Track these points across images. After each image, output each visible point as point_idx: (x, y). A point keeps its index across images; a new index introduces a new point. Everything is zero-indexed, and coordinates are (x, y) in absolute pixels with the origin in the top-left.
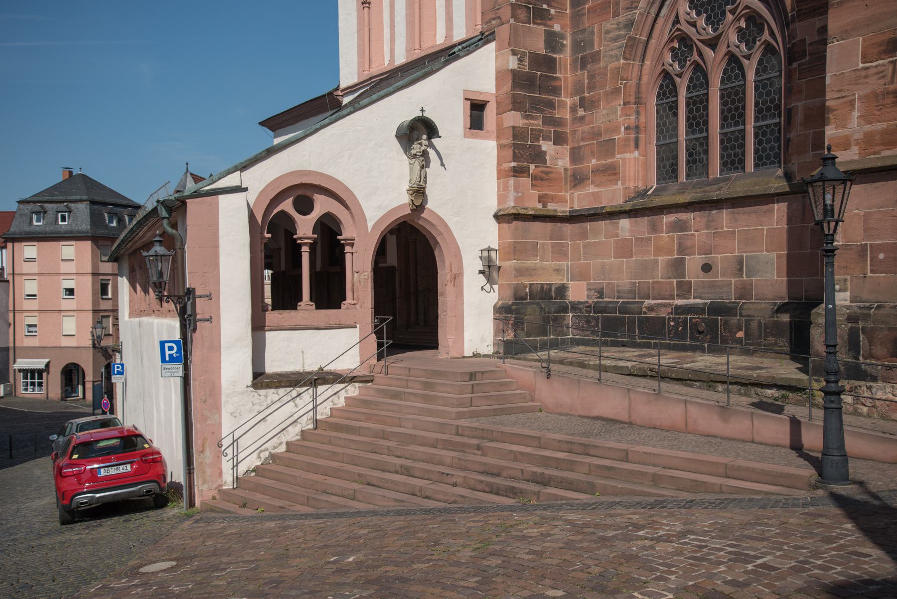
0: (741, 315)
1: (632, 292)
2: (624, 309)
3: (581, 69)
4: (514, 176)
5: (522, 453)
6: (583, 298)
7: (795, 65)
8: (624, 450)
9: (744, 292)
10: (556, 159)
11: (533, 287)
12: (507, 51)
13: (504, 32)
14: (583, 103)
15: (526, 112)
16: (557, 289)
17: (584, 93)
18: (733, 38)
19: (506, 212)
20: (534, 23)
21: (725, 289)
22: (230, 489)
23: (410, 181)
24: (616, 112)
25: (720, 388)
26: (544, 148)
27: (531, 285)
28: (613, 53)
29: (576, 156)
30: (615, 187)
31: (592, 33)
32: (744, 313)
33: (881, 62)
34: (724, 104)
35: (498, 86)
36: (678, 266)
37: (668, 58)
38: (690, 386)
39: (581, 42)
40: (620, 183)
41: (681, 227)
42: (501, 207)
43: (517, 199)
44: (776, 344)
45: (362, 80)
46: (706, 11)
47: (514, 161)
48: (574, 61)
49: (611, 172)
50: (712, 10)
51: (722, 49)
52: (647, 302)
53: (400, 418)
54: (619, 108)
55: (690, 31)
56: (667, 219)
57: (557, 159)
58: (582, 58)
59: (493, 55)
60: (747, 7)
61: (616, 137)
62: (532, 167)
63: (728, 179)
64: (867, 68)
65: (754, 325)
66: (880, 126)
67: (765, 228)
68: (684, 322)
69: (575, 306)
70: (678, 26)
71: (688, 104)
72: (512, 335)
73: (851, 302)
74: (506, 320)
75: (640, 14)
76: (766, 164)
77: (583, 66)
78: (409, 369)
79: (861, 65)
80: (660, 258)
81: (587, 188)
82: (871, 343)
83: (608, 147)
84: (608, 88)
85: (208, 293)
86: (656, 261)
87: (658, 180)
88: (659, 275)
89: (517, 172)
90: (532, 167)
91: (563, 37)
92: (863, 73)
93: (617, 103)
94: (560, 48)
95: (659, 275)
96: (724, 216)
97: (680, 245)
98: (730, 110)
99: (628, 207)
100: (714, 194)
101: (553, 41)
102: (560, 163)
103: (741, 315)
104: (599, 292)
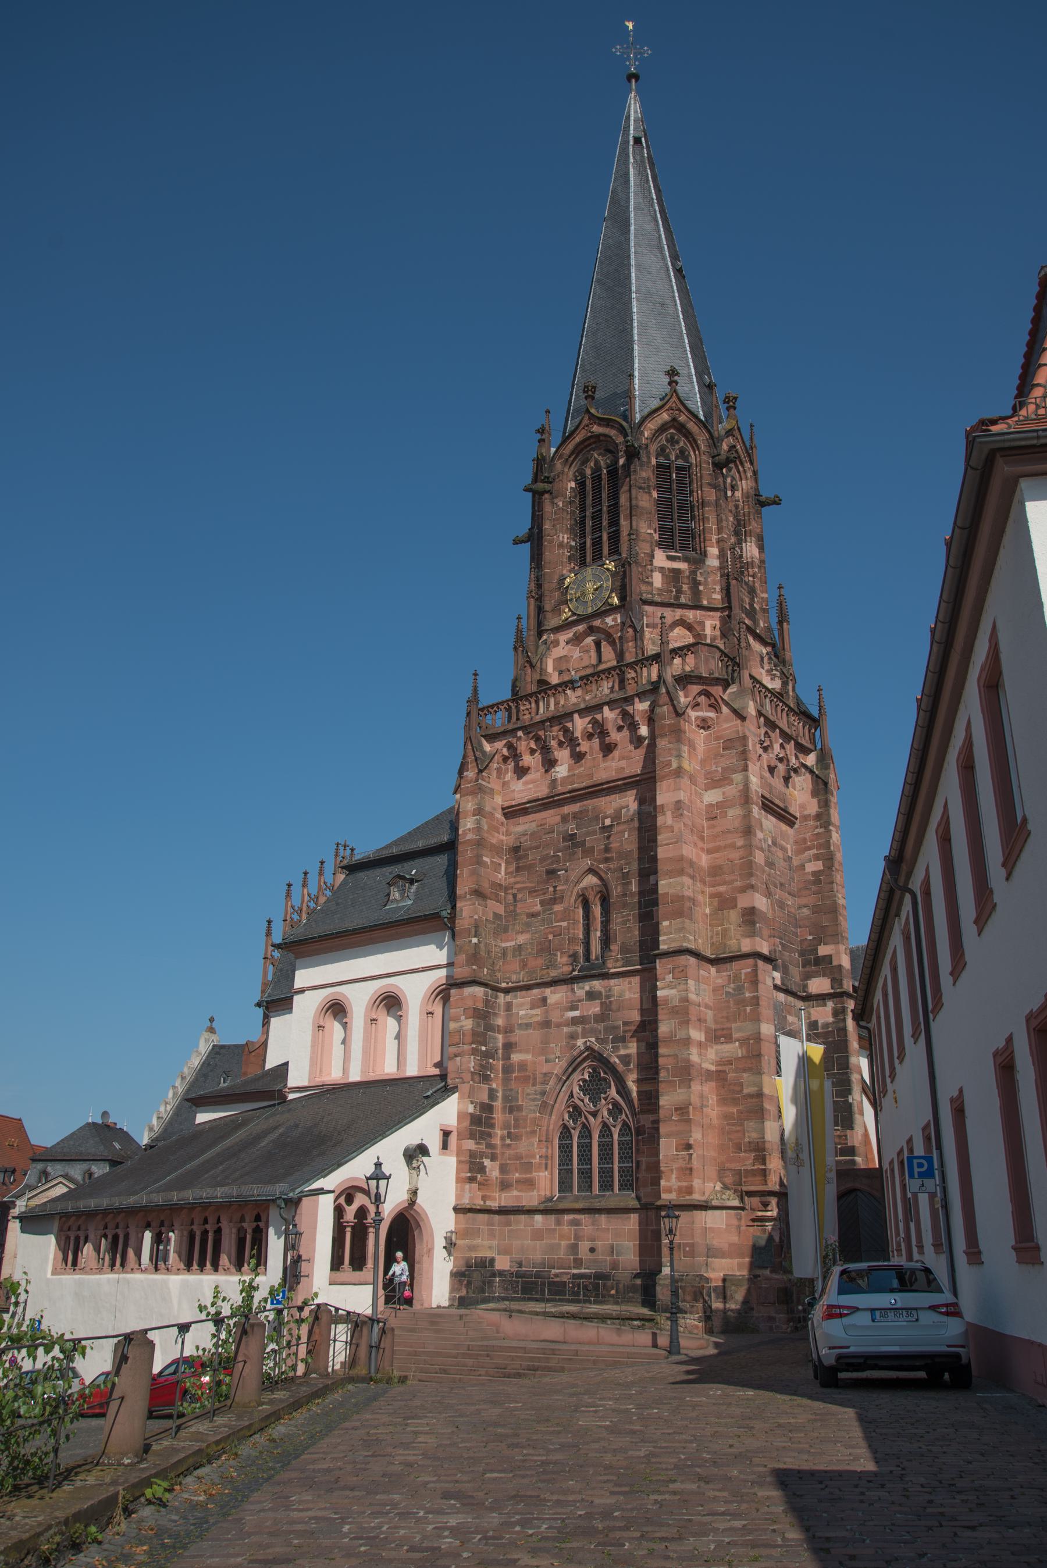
14: (509, 1135)
18: (606, 1114)
24: (533, 1145)
28: (532, 1108)
37: (566, 1117)
46: (589, 1094)
48: (504, 1108)
51: (600, 1119)
55: (580, 1104)
58: (510, 1106)
77: (511, 1112)
91: (497, 1091)
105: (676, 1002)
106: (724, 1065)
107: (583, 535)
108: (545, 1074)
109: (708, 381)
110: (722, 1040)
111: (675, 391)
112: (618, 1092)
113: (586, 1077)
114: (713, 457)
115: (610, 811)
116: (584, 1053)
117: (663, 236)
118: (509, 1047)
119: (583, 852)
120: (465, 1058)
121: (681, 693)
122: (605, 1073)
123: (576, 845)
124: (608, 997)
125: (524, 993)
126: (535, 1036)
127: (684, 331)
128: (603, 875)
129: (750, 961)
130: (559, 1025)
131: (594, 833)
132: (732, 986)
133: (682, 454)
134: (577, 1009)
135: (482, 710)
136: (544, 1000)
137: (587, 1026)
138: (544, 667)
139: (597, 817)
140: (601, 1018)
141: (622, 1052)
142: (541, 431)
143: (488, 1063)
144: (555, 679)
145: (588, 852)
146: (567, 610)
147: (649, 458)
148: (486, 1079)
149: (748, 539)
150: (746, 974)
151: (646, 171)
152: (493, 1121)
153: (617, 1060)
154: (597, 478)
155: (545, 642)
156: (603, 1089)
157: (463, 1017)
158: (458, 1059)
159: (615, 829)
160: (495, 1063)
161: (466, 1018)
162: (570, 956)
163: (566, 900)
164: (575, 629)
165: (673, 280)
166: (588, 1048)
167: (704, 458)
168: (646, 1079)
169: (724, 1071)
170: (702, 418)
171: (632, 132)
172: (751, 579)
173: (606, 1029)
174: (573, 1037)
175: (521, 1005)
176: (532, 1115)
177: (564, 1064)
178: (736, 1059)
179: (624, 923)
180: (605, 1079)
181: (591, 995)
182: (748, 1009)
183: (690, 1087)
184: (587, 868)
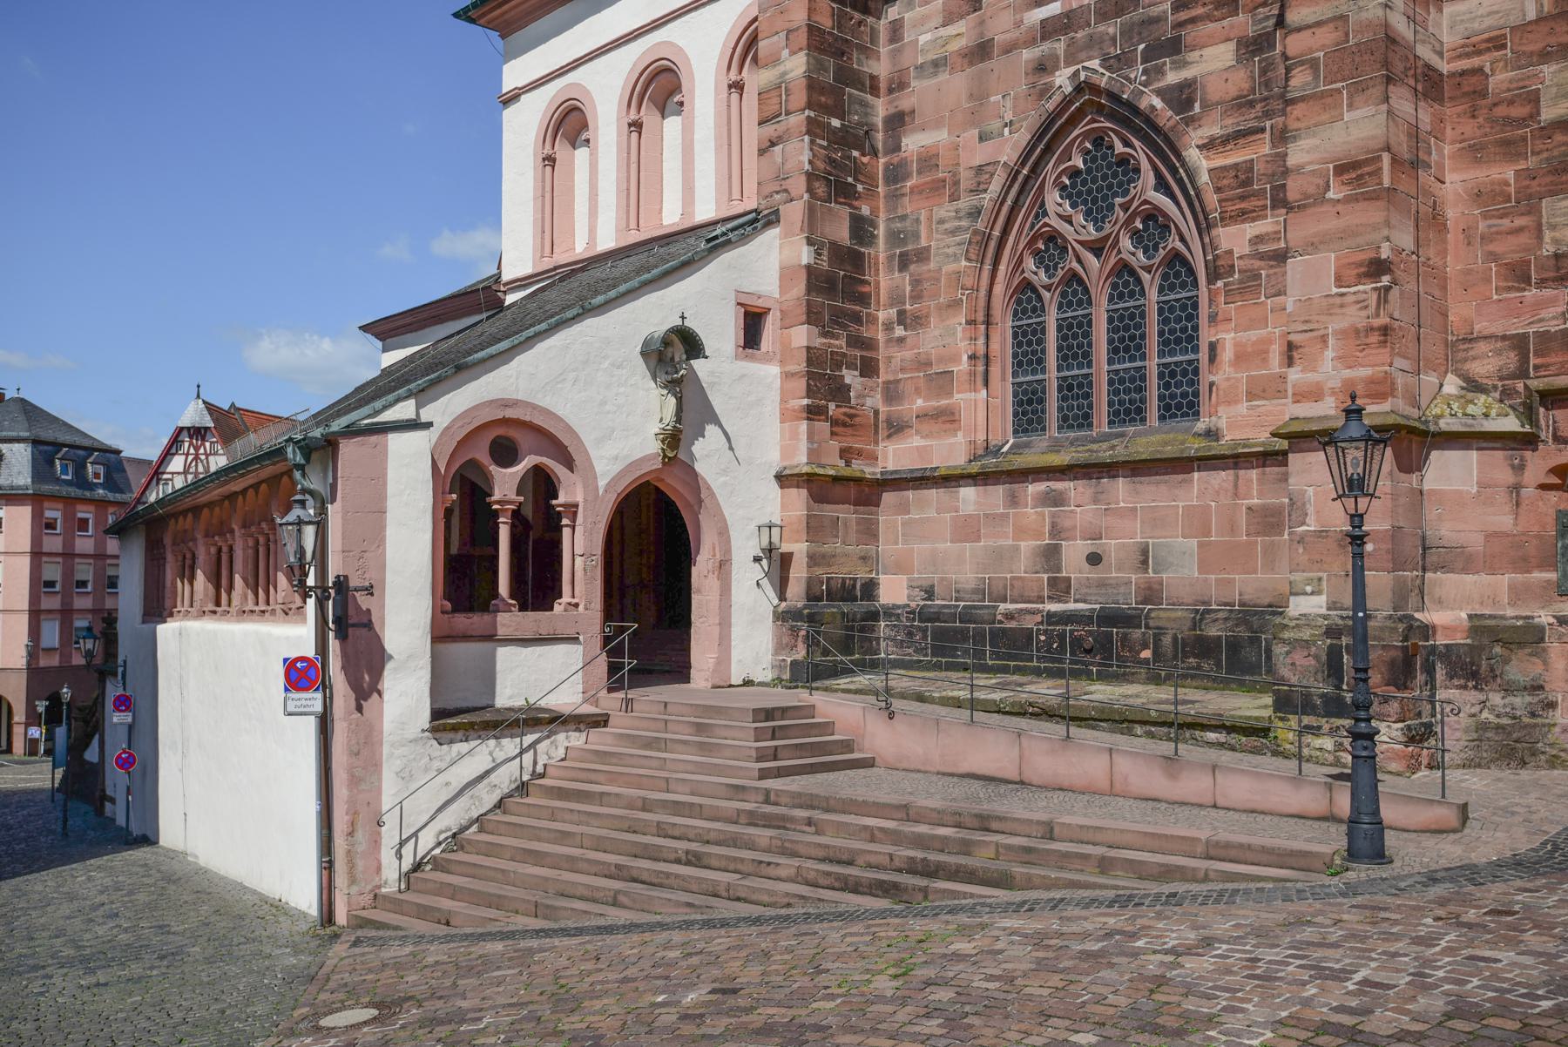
0: (1147, 627)
1: (979, 592)
2: (967, 616)
3: (900, 270)
4: (808, 419)
5: (881, 829)
6: (901, 599)
7: (1220, 284)
8: (1039, 823)
9: (1151, 594)
11: (832, 582)
13: (794, 212)
14: (902, 318)
15: (823, 327)
16: (862, 585)
17: (904, 303)
19: (796, 471)
20: (836, 202)
21: (1122, 590)
22: (394, 893)
23: (661, 420)
24: (954, 334)
25: (1139, 730)
26: (848, 380)
27: (828, 579)
28: (950, 251)
30: (952, 440)
31: (918, 221)
32: (1151, 623)
33: (1361, 288)
34: (1113, 330)
35: (783, 288)
36: (1051, 555)
37: (1030, 263)
38: (1093, 728)
39: (900, 232)
40: (960, 434)
41: (1056, 500)
42: (786, 463)
43: (813, 454)
44: (1199, 667)
45: (540, 270)
46: (1085, 202)
47: (808, 397)
48: (890, 258)
49: (947, 418)
50: (1094, 201)
52: (1003, 607)
53: (667, 780)
54: (960, 329)
56: (1034, 489)
57: (864, 396)
58: (901, 255)
59: (777, 242)
60: (1146, 202)
61: (955, 369)
62: (832, 406)
63: (1122, 435)
64: (1343, 295)
65: (1167, 640)
66: (1364, 372)
67: (1181, 504)
68: (1062, 636)
69: (890, 612)
70: (1046, 220)
71: (1059, 328)
72: (804, 653)
73: (1329, 609)
74: (794, 631)
75: (991, 200)
76: (1176, 416)
78: (666, 704)
79: (1335, 290)
80: (1022, 544)
81: (910, 440)
83: (942, 383)
84: (941, 300)
85: (367, 584)
86: (1017, 548)
87: (1015, 432)
89: (813, 413)
90: (832, 406)
91: (874, 225)
92: (1338, 300)
93: (956, 320)
94: (871, 239)
95: (1023, 566)
96: (1120, 488)
97: (1054, 525)
98: (1122, 340)
99: (975, 468)
101: (861, 229)
102: (869, 402)
103: (1147, 627)
104: (926, 592)
106: (1479, 53)
108: (979, 169)
112: (1162, 185)
113: (1078, 162)
116: (1071, 102)
118: (898, 122)
122: (1127, 144)
130: (1009, 49)
137: (1080, 34)
141: (1172, 78)
143: (849, 157)
148: (843, 192)
152: (865, 289)
153: (1157, 102)
156: (1120, 185)
160: (865, 160)
161: (793, 53)
166: (1079, 89)
169: (1479, 71)
173: (1127, 32)
174: (1043, 67)
176: (950, 267)
177: (1023, 137)
178: (1523, 29)
180: (1123, 161)
183: (1387, 99)
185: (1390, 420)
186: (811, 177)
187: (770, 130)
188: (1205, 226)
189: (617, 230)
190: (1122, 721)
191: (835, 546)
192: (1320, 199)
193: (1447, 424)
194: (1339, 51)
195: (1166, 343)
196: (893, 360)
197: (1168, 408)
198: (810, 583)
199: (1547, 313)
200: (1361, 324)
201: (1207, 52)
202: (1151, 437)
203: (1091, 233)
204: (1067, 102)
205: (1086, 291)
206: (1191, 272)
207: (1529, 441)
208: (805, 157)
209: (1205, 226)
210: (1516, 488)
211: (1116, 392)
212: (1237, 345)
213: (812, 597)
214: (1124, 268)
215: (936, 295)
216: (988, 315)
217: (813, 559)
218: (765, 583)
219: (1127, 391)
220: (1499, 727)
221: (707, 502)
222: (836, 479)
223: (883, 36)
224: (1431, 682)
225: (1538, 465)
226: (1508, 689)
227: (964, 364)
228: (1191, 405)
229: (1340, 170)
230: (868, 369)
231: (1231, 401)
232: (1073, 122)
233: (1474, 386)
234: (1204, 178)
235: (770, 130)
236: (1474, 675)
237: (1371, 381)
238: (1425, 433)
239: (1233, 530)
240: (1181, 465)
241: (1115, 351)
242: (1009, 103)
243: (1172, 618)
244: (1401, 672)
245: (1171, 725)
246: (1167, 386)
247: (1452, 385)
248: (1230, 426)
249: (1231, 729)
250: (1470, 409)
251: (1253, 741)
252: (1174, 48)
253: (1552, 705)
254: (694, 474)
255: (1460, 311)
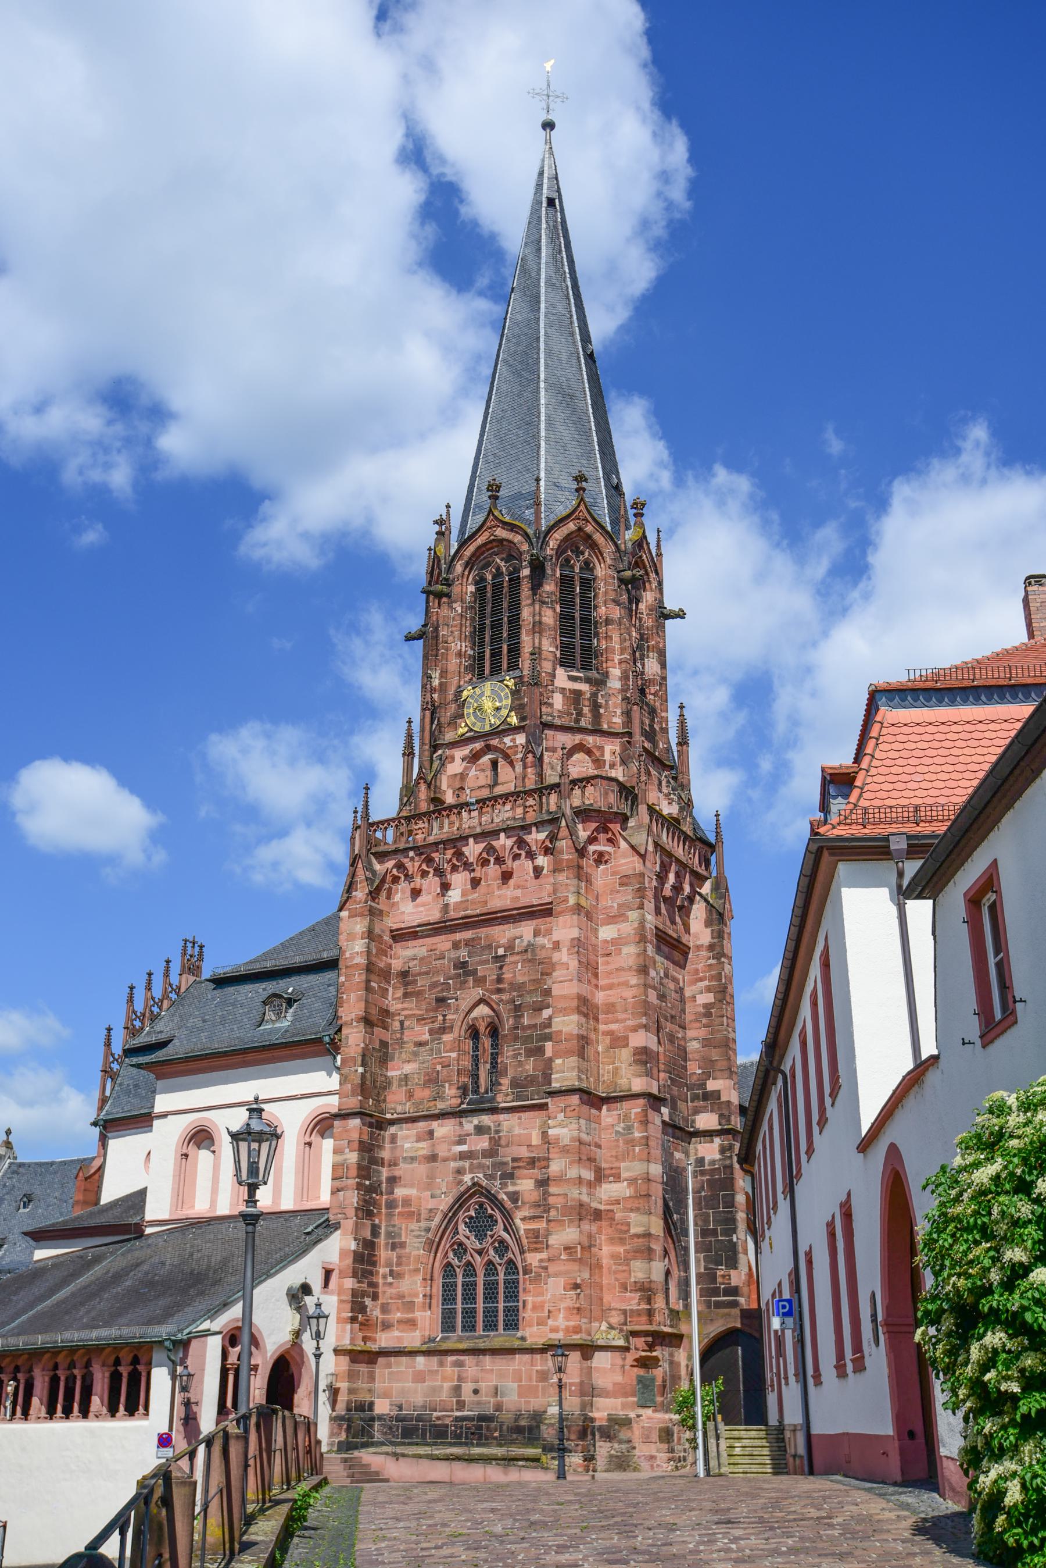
1: (424, 1407)
2: (419, 1419)
6: (386, 1411)
9: (498, 1408)
10: (371, 1311)
12: (351, 1238)
13: (349, 1224)
14: (391, 1273)
29: (385, 1309)
35: (340, 1258)
36: (457, 1390)
37: (451, 1254)
41: (460, 1364)
43: (352, 1339)
48: (387, 1244)
49: (412, 1323)
52: (435, 1414)
56: (450, 1359)
62: (360, 1316)
63: (488, 1336)
65: (505, 1427)
66: (572, 1323)
69: (380, 1418)
74: (340, 1426)
82: (569, 1432)
86: (442, 1387)
88: (445, 1395)
89: (353, 1320)
90: (360, 1316)
91: (380, 1228)
95: (445, 1395)
96: (487, 1359)
97: (459, 1376)
99: (424, 1348)
100: (482, 1346)
101: (375, 1231)
102: (375, 1313)
105: (567, 1141)
107: (482, 644)
108: (430, 1210)
109: (616, 481)
110: (611, 1179)
111: (582, 499)
112: (506, 1230)
113: (472, 1213)
114: (619, 572)
115: (504, 941)
117: (575, 317)
118: (393, 1180)
119: (474, 981)
120: (349, 1193)
121: (580, 826)
122: (493, 1209)
123: (467, 974)
124: (497, 1132)
125: (409, 1125)
126: (421, 1170)
127: (594, 428)
128: (495, 1006)
129: (641, 1102)
130: (445, 1160)
131: (486, 962)
132: (622, 1125)
133: (587, 566)
134: (465, 1143)
135: (372, 825)
136: (431, 1133)
137: (475, 1161)
138: (438, 784)
139: (489, 947)
140: (490, 1153)
142: (440, 522)
143: (371, 1198)
144: (450, 799)
145: (480, 981)
146: (463, 724)
147: (554, 571)
148: (369, 1214)
149: (651, 654)
150: (636, 1114)
151: (558, 239)
153: (505, 1197)
154: (497, 587)
155: (440, 757)
157: (347, 1150)
158: (341, 1193)
159: (508, 960)
162: (458, 1088)
163: (456, 1030)
164: (471, 747)
165: (584, 368)
166: (474, 1184)
167: (610, 572)
168: (535, 1217)
170: (609, 529)
171: (545, 191)
172: (652, 697)
173: (494, 1165)
174: (459, 1172)
175: (407, 1137)
177: (450, 1200)
179: (515, 1056)
180: (491, 1216)
181: (480, 1130)
182: (637, 1149)
184: (478, 997)
185: (580, 1342)
186: (357, 1209)
187: (338, 1184)
188: (522, 1252)
189: (231, 1205)
190: (487, 1460)
191: (359, 1384)
192: (559, 1259)
193: (600, 1343)
194: (564, 1207)
195: (506, 1297)
196: (386, 1293)
197: (507, 1325)
198: (349, 1402)
199: (633, 1302)
200: (571, 1306)
201: (524, 1181)
202: (500, 1338)
203: (479, 1246)
204: (469, 1189)
205: (474, 1270)
206: (516, 1268)
207: (627, 1349)
208: (355, 1200)
209: (522, 1252)
210: (623, 1366)
211: (486, 1316)
212: (533, 1302)
213: (349, 1410)
214: (490, 1263)
215: (408, 1265)
216: (432, 1276)
217: (351, 1391)
218: (327, 1403)
219: (491, 1316)
220: (617, 1457)
221: (306, 1363)
222: (361, 1352)
223: (387, 1140)
224: (594, 1438)
225: (631, 1357)
226: (620, 1442)
227: (420, 1299)
228: (516, 1325)
229: (565, 1249)
230: (375, 1297)
231: (531, 1326)
232: (471, 1196)
233: (611, 1327)
234: (522, 1232)
235: (338, 1184)
236: (609, 1437)
237: (574, 1327)
238: (592, 1346)
239: (530, 1380)
240: (511, 1351)
241: (486, 1298)
242: (445, 1184)
243: (506, 1417)
244: (583, 1434)
245: (504, 1459)
246: (507, 1316)
247: (604, 1326)
248: (531, 1336)
249: (527, 1460)
250: (609, 1336)
251: (535, 1464)
252: (511, 1176)
253: (634, 1448)
254: (302, 1350)
255: (607, 1298)
